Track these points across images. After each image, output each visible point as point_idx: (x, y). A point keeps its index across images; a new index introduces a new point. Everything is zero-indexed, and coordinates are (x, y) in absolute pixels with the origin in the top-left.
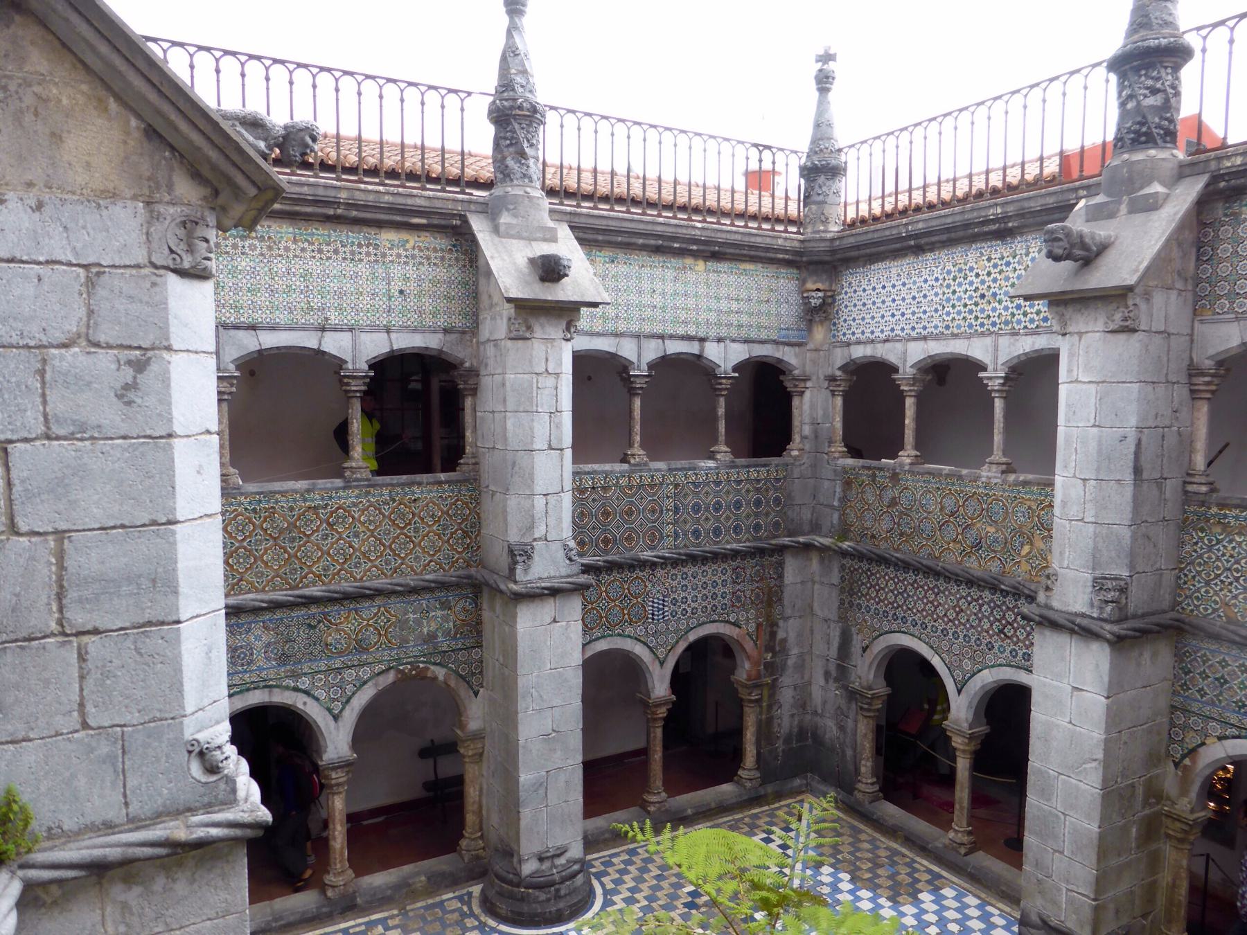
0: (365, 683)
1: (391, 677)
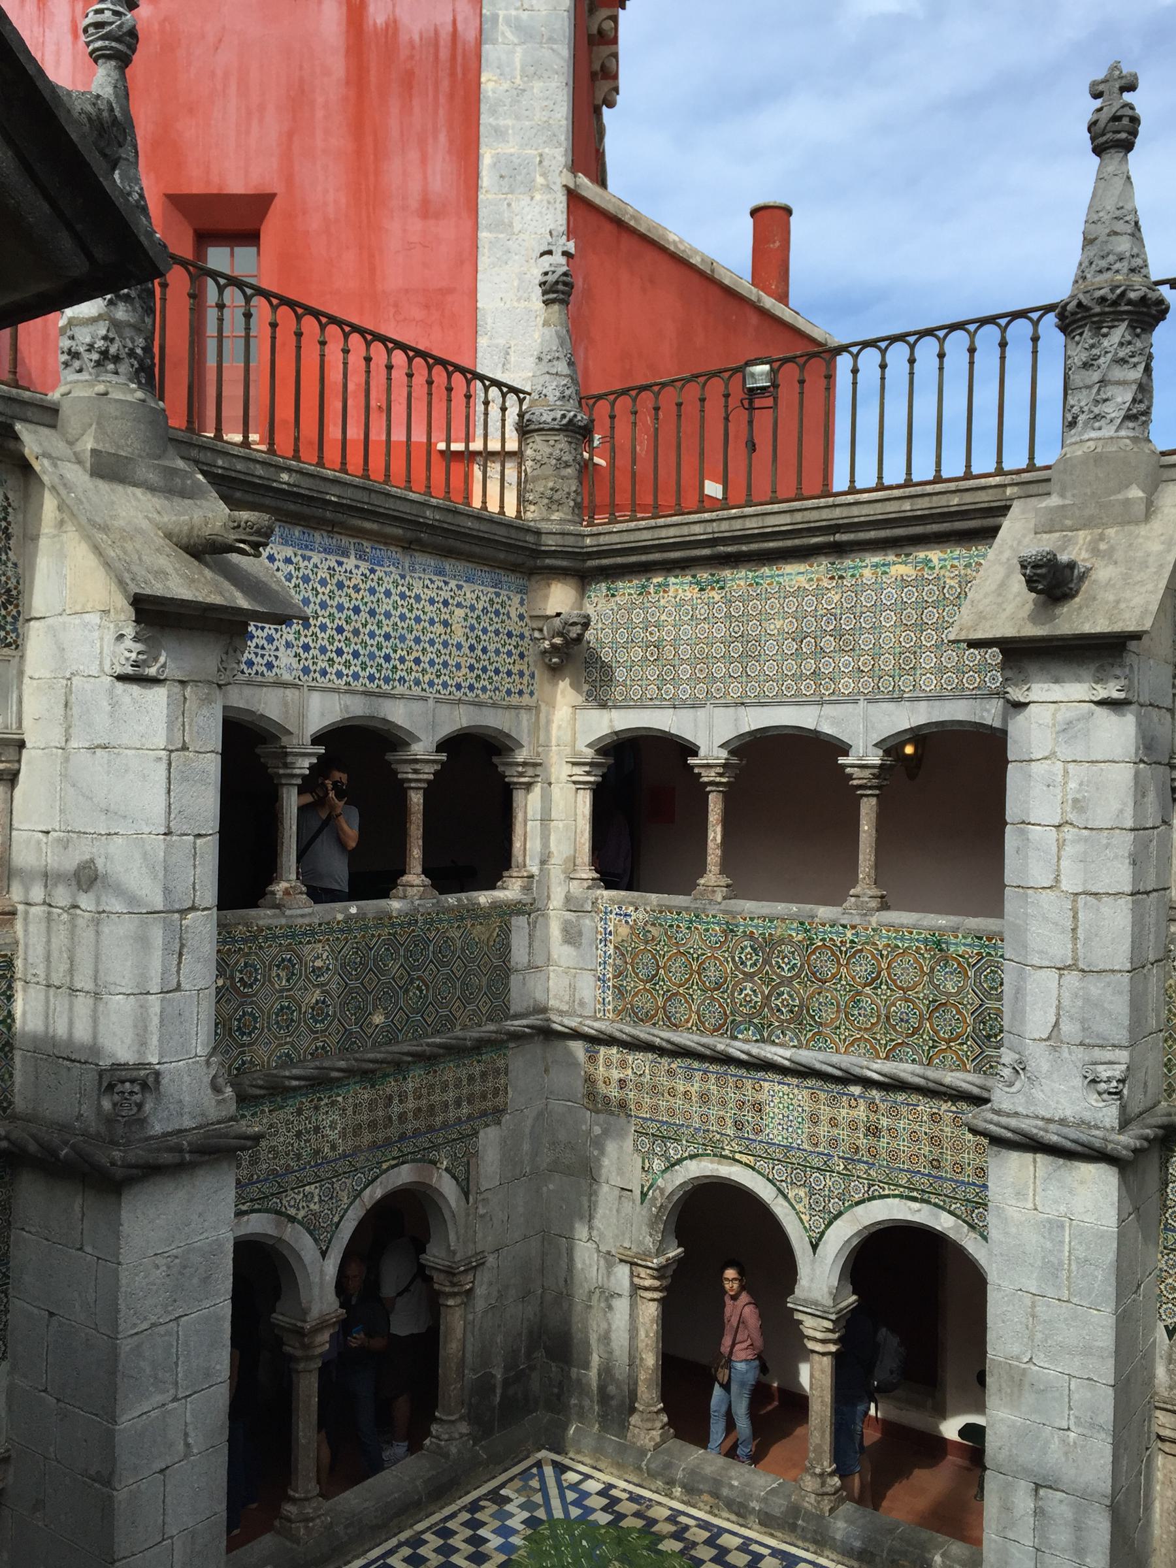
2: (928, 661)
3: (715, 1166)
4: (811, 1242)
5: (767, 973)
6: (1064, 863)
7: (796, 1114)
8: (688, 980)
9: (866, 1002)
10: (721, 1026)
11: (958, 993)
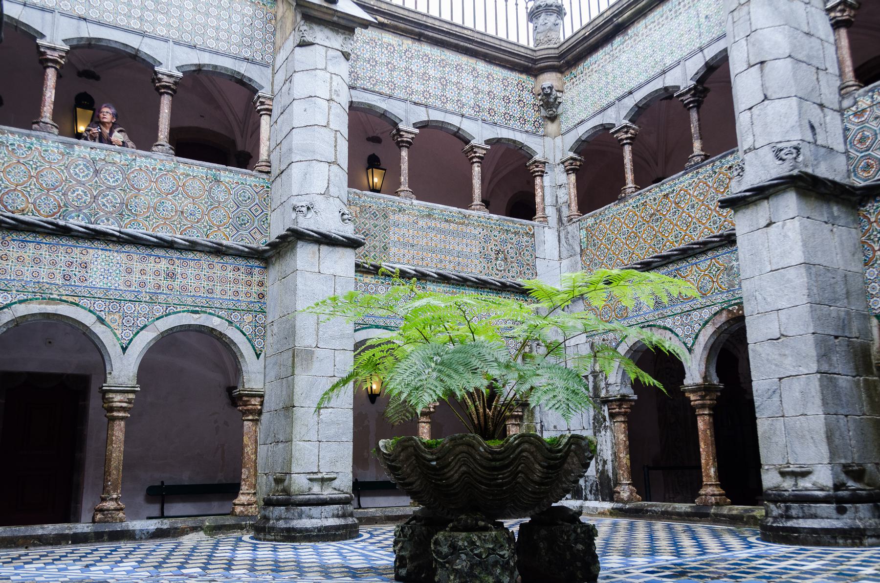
0: (707, 322)
1: (724, 317)
2: (211, 32)
3: (43, 306)
4: (122, 347)
5: (96, 182)
6: (331, 117)
7: (114, 268)
8: (25, 182)
9: (168, 204)
10: (55, 214)
11: (224, 202)
